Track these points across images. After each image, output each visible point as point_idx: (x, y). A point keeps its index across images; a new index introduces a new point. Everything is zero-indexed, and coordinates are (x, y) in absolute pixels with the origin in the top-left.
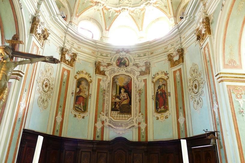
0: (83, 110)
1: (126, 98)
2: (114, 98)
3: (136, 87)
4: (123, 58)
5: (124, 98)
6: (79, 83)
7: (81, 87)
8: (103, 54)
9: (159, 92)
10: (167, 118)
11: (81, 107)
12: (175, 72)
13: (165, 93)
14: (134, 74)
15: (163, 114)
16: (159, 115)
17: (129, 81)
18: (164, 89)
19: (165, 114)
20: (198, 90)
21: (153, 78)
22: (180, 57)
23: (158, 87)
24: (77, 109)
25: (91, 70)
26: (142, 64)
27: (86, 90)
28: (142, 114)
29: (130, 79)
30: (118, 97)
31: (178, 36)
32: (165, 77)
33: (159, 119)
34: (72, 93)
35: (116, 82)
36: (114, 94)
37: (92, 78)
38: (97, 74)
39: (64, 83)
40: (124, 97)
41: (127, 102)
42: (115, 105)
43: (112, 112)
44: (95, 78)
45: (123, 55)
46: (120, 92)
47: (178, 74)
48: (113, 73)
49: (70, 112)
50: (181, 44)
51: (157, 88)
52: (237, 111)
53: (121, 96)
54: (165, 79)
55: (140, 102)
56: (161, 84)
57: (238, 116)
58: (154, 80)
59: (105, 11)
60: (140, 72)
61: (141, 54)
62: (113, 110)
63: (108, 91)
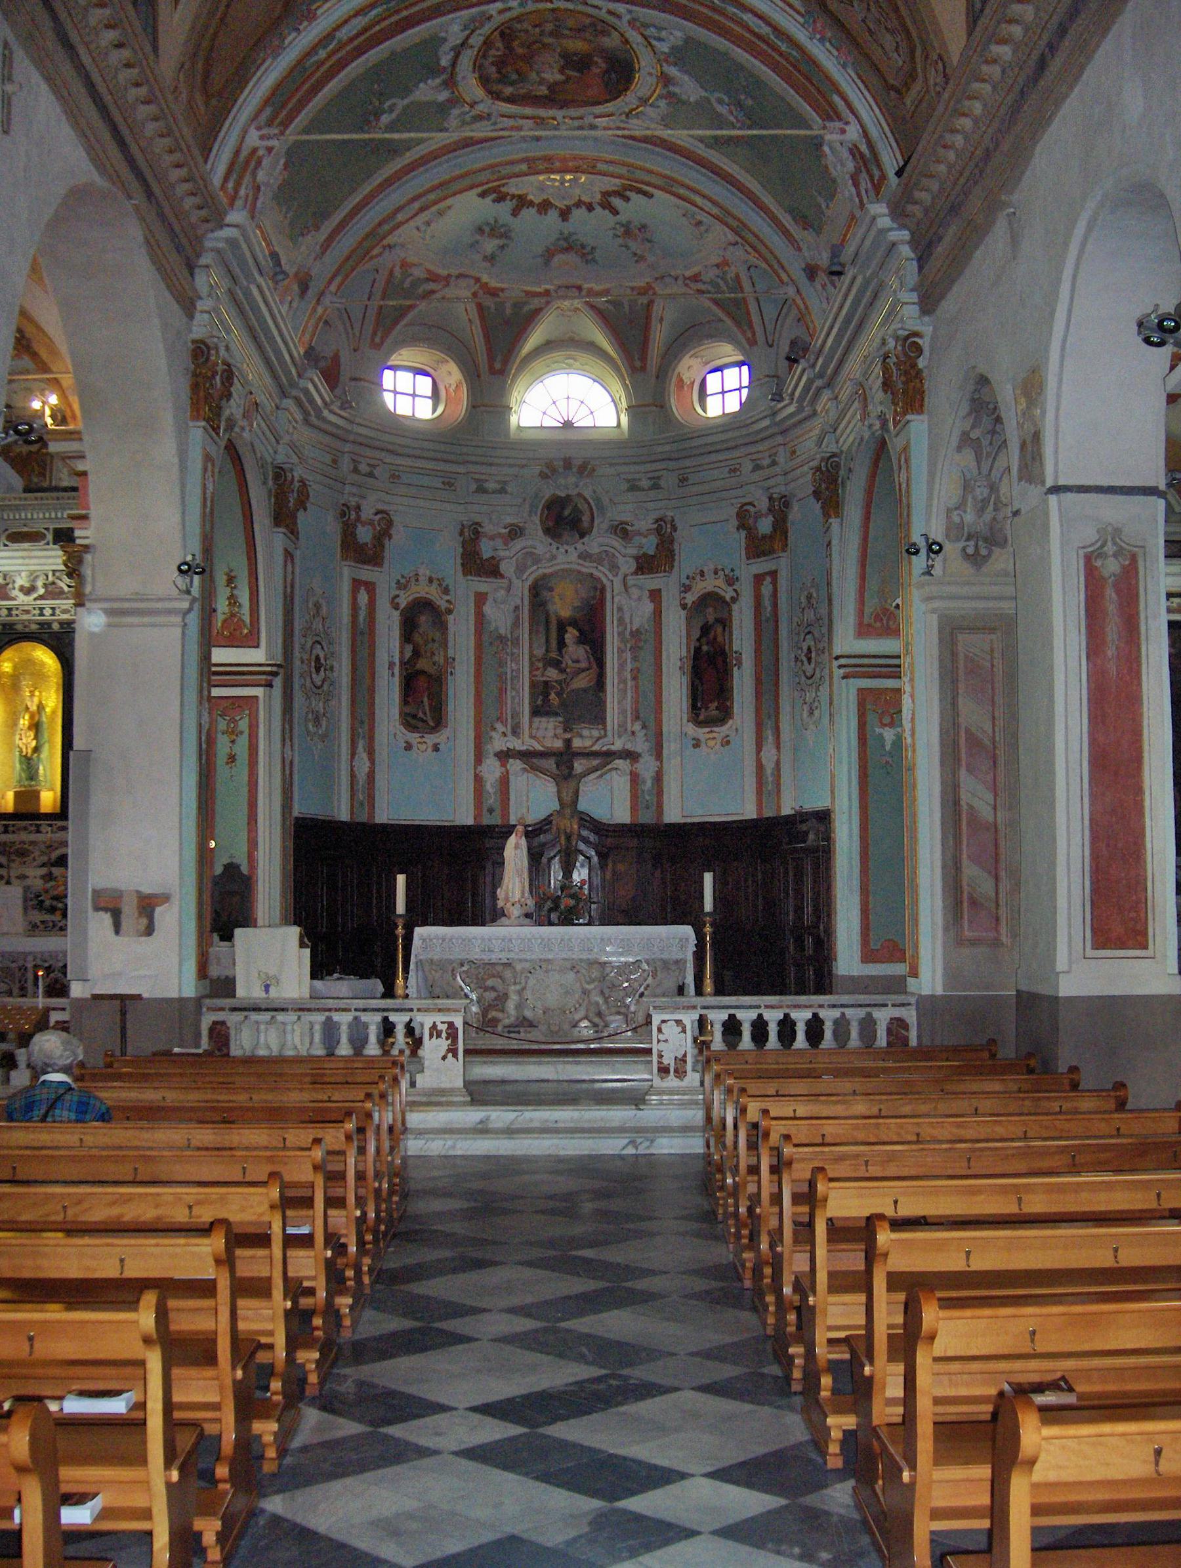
0: (432, 724)
1: (583, 665)
2: (540, 665)
3: (621, 621)
4: (568, 496)
5: (578, 665)
6: (409, 626)
7: (417, 638)
8: (487, 485)
9: (705, 648)
10: (728, 743)
11: (425, 714)
12: (758, 579)
13: (723, 653)
14: (614, 567)
15: (715, 729)
16: (702, 733)
17: (594, 598)
18: (720, 639)
19: (723, 730)
21: (687, 589)
23: (702, 628)
24: (413, 722)
25: (448, 562)
26: (645, 523)
27: (436, 645)
28: (644, 727)
29: (599, 586)
30: (556, 664)
32: (728, 595)
33: (703, 745)
34: (391, 665)
35: (543, 604)
36: (539, 652)
37: (452, 593)
38: (469, 577)
39: (362, 633)
40: (578, 661)
41: (590, 681)
42: (546, 695)
43: (536, 720)
44: (465, 588)
45: (565, 485)
46: (562, 644)
47: (766, 589)
48: (529, 563)
49: (392, 737)
51: (697, 633)
53: (567, 661)
54: (728, 598)
55: (635, 678)
56: (711, 615)
58: (690, 598)
59: (489, 302)
60: (637, 558)
61: (640, 480)
62: (536, 712)
63: (516, 642)
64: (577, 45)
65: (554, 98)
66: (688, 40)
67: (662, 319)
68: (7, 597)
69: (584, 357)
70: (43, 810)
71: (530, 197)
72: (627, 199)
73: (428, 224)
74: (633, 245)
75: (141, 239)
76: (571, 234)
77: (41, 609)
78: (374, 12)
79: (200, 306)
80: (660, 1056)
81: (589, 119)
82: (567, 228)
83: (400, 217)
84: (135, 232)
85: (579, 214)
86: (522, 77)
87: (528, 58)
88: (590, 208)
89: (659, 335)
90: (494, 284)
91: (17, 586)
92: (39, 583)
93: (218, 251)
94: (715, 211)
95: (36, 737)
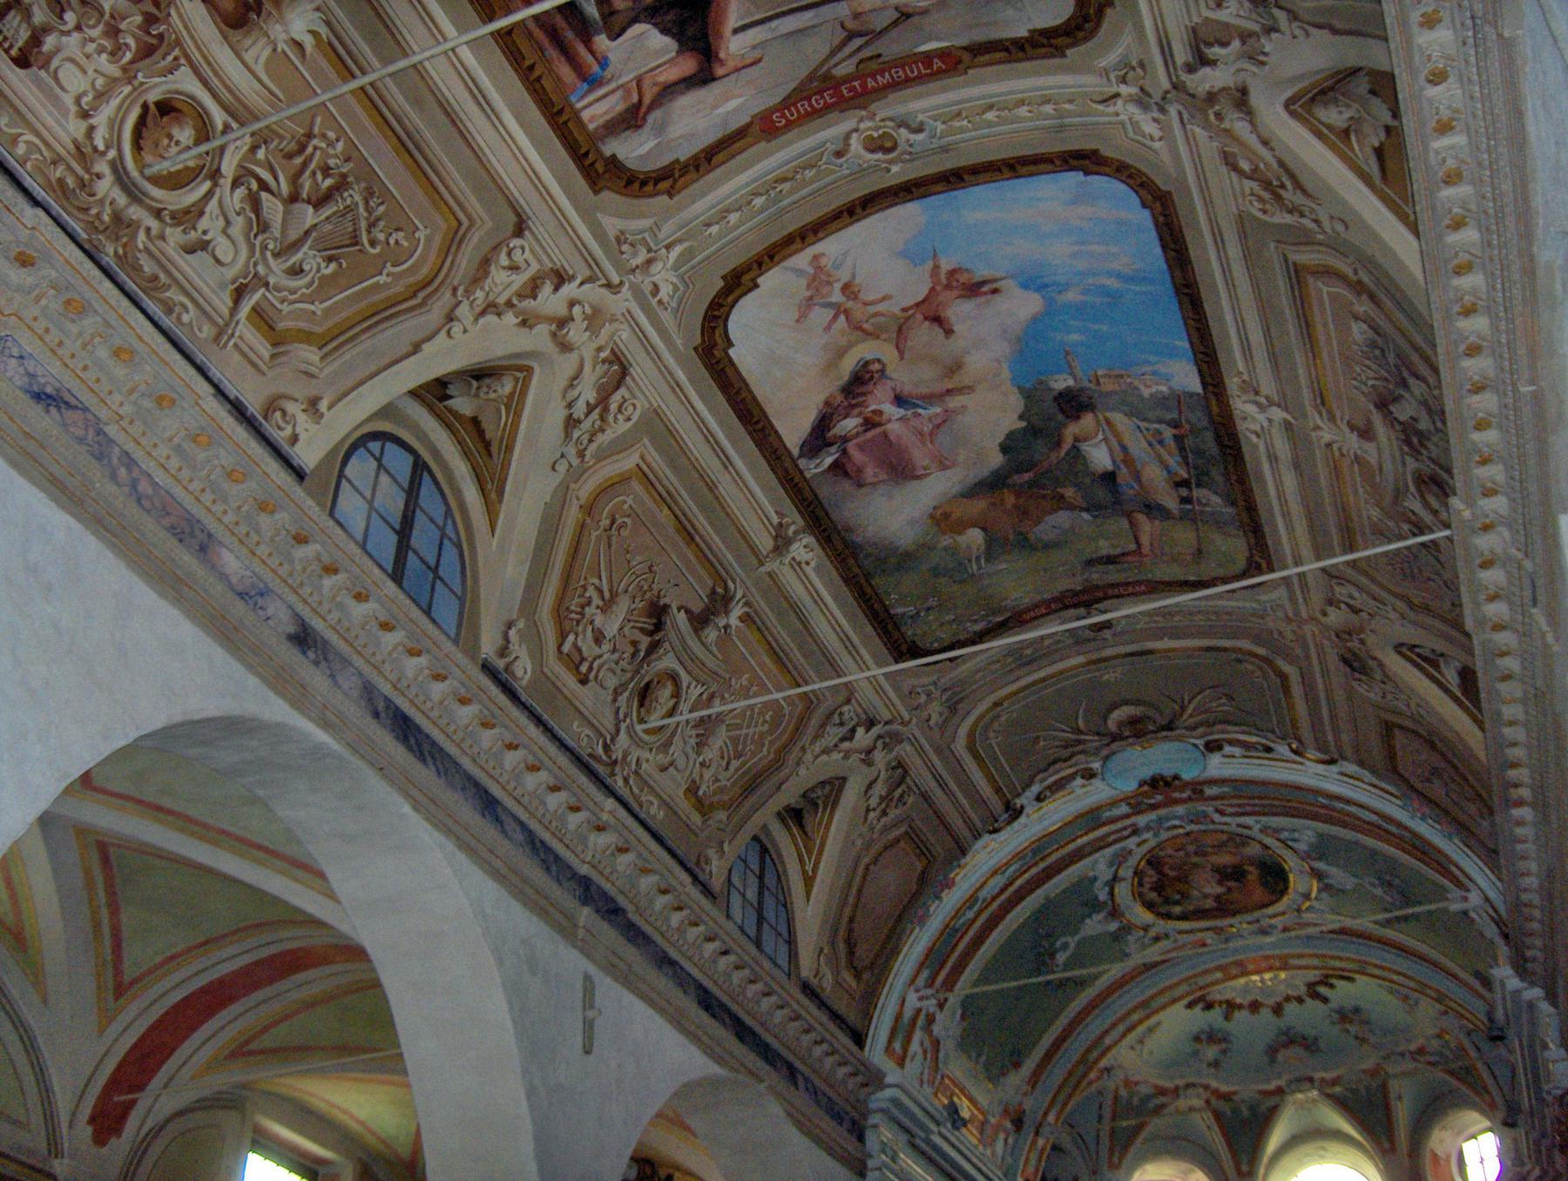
64: (1225, 859)
65: (1223, 908)
66: (1321, 836)
67: (1400, 1098)
69: (1334, 1146)
71: (1238, 1001)
72: (1332, 986)
73: (1141, 1042)
74: (1353, 1029)
75: (782, 1114)
76: (1289, 1029)
78: (1012, 869)
79: (871, 1163)
81: (1265, 922)
82: (1282, 1023)
83: (1108, 1041)
84: (775, 1108)
85: (1291, 1008)
86: (1185, 896)
87: (1183, 879)
88: (1300, 1000)
89: (1403, 1114)
90: (1224, 1088)
93: (882, 1110)
94: (1412, 984)
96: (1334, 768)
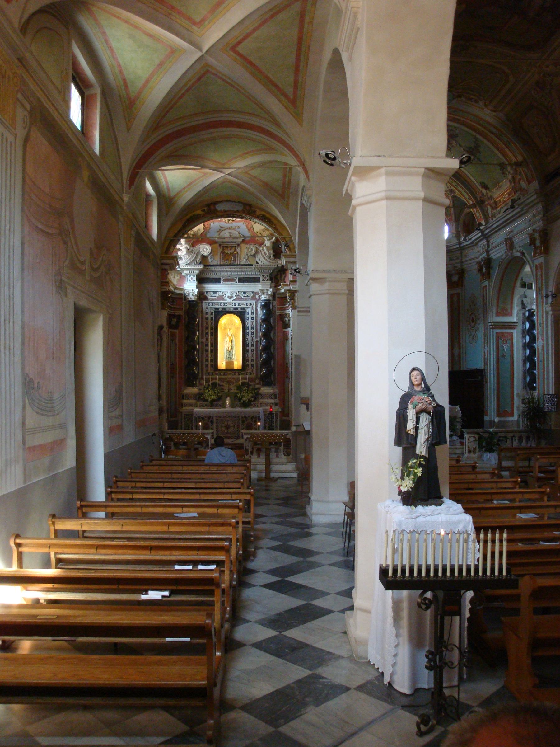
20: (475, 324)
22: (459, 278)
31: (459, 252)
50: (462, 262)
52: (501, 354)
57: (501, 359)
68: (224, 300)
70: (235, 368)
77: (235, 304)
80: (469, 447)
91: (226, 296)
92: (234, 295)
95: (232, 344)
96: (494, 113)
